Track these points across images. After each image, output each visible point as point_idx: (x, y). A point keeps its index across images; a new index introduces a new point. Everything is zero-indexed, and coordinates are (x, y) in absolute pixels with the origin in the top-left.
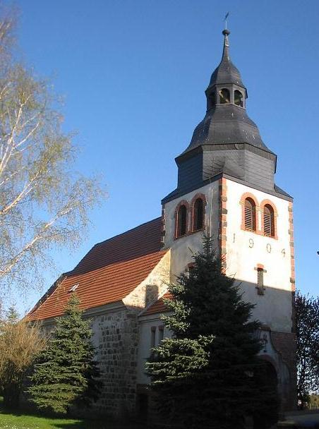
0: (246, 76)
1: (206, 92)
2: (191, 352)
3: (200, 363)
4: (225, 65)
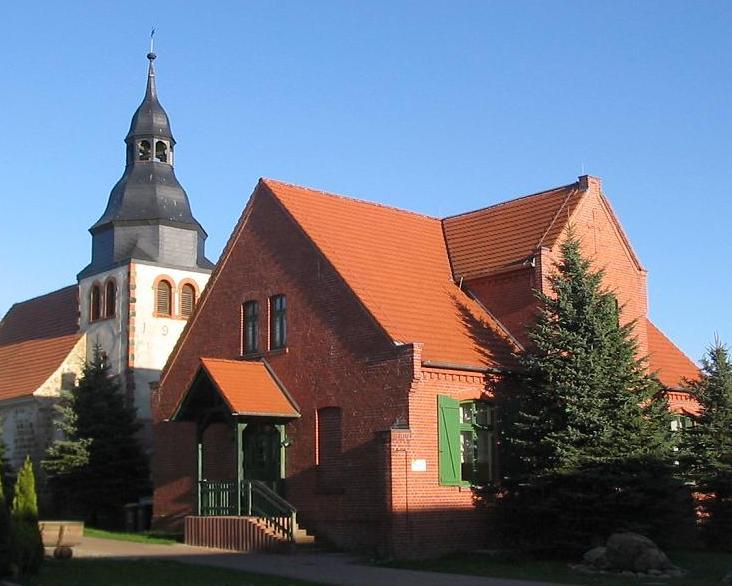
0: (178, 116)
1: (14, 305)
2: (75, 452)
3: (82, 461)
4: (149, 105)
